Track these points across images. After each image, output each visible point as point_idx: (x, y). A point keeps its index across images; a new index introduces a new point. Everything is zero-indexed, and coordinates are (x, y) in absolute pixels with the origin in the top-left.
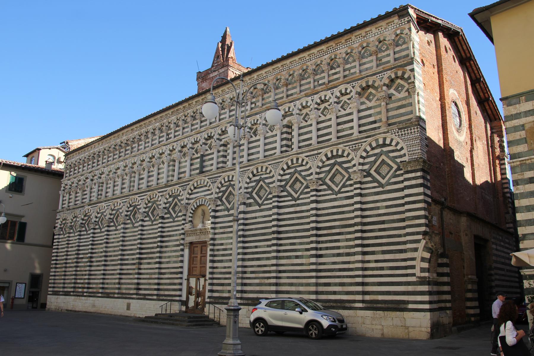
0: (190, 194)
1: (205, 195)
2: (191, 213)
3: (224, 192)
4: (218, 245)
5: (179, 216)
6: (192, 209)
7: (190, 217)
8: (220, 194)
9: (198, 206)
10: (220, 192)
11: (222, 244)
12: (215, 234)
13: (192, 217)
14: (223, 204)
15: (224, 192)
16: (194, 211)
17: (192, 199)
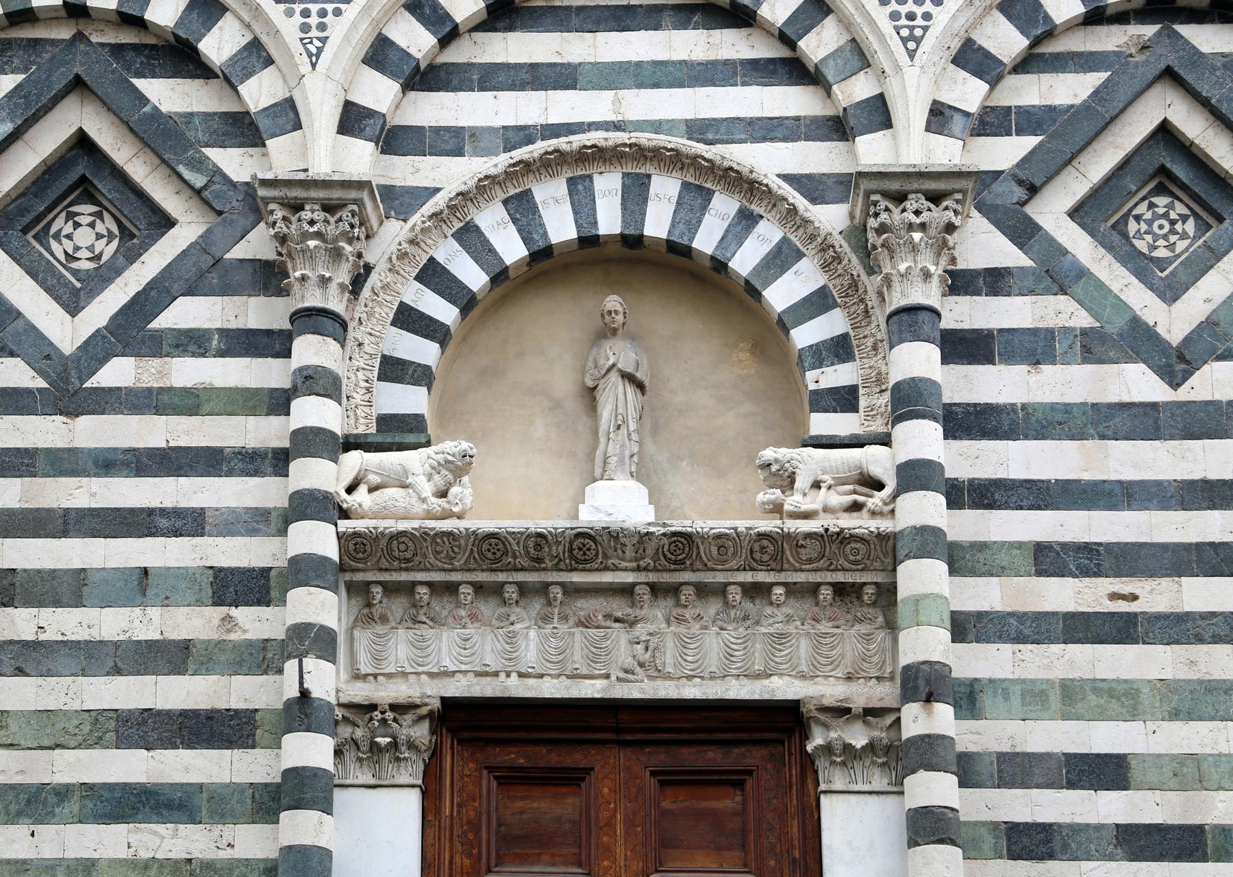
0: (423, 78)
1: (699, 129)
2: (408, 319)
3: (1064, 135)
4: (1017, 770)
5: (192, 342)
6: (434, 276)
7: (394, 370)
8: (1005, 152)
9: (542, 255)
10: (992, 122)
11: (1106, 772)
12: (964, 627)
13: (419, 375)
14: (1057, 274)
15: (1064, 135)
16: (466, 302)
17: (450, 141)
